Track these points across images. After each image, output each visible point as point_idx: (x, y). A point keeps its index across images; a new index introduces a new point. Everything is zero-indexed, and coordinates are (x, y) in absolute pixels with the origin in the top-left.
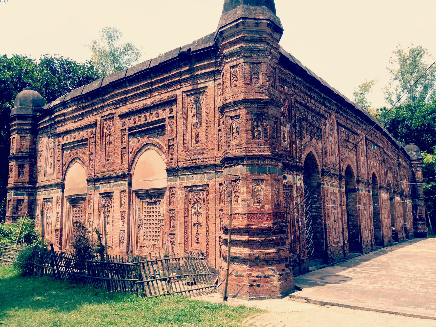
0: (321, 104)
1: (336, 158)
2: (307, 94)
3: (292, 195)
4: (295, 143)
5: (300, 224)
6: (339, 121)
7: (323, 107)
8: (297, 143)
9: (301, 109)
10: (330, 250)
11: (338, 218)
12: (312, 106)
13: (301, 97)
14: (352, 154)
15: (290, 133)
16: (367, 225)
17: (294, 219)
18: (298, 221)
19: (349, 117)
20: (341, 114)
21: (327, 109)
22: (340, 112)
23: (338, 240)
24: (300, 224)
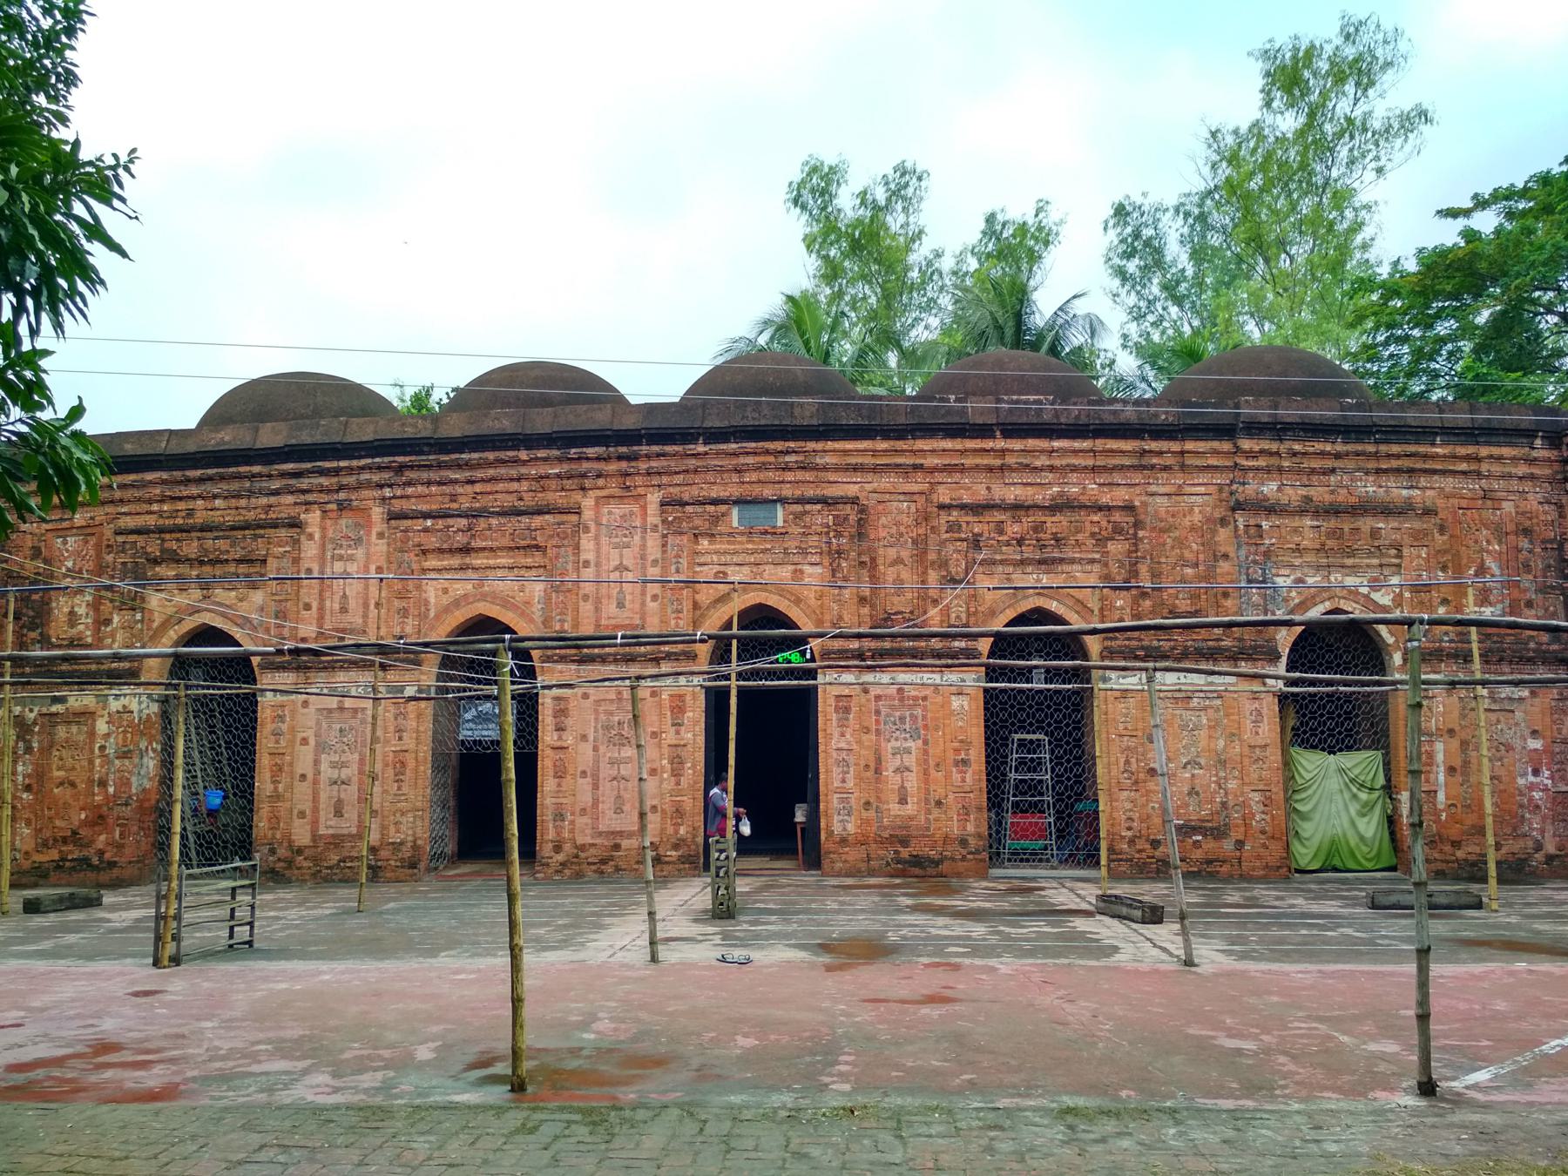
0: (276, 493)
1: (365, 616)
2: (180, 499)
3: (92, 734)
4: (108, 622)
5: (111, 790)
6: (398, 505)
7: (290, 499)
8: (116, 619)
9: (140, 540)
10: (273, 851)
11: (361, 772)
12: (216, 517)
13: (151, 513)
14: (503, 585)
15: (95, 606)
16: (630, 794)
17: (91, 781)
18: (103, 783)
19: (479, 474)
20: (409, 484)
21: (309, 497)
22: (412, 475)
23: (354, 831)
24: (111, 790)
